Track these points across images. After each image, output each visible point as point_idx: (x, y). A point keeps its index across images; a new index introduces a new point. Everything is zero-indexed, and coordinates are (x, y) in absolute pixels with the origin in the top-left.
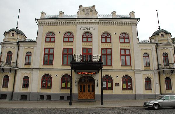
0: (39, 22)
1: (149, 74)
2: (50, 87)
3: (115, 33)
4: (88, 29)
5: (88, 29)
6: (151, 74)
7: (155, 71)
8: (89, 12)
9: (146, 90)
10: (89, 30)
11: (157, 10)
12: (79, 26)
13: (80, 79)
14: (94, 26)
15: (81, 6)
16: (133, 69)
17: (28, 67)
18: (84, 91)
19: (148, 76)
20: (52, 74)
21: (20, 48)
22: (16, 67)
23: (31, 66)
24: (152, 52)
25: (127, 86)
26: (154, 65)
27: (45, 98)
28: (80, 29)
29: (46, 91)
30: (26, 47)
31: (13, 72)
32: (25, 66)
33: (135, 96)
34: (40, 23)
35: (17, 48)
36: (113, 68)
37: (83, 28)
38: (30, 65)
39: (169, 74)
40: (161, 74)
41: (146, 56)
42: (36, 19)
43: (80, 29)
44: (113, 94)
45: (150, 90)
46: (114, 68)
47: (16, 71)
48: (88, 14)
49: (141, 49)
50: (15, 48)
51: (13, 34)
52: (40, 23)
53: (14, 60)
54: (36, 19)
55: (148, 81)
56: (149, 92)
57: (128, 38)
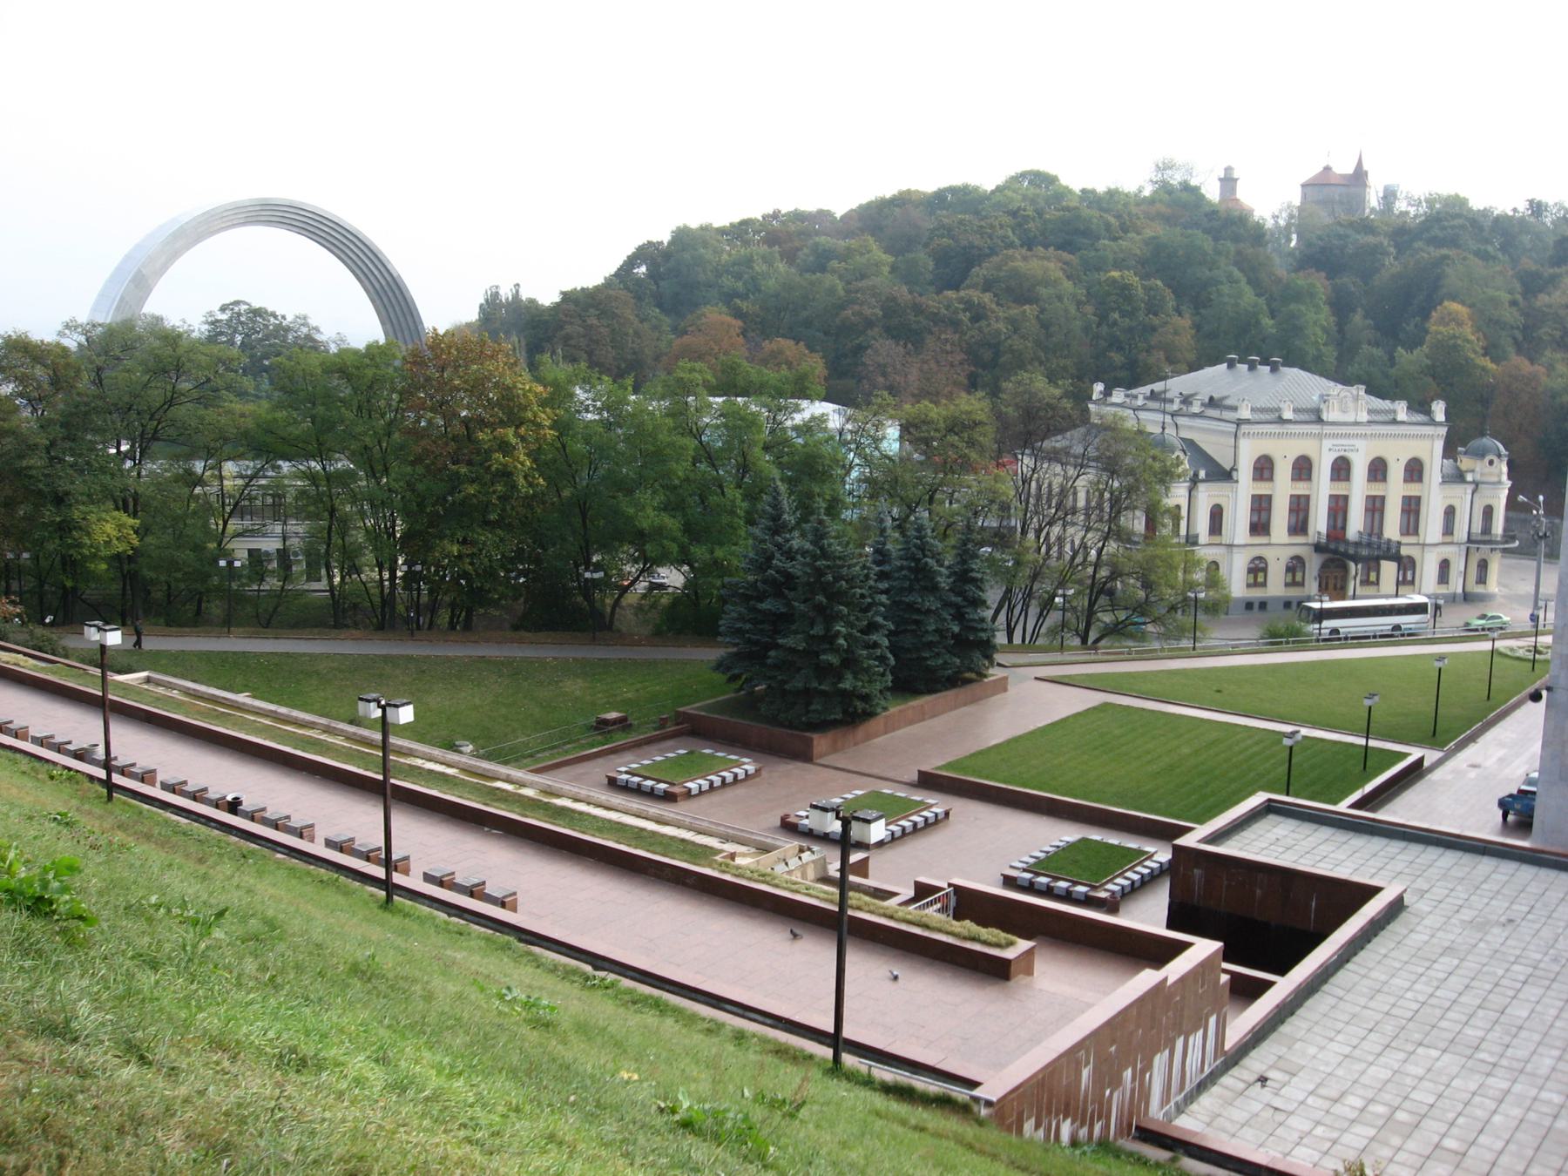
1: (1447, 552)
2: (1264, 584)
10: (1347, 454)
12: (1327, 443)
14: (1359, 443)
18: (1327, 588)
19: (1445, 556)
20: (1269, 554)
23: (1226, 539)
26: (1461, 533)
27: (1256, 606)
29: (1257, 594)
40: (1472, 551)
41: (1450, 512)
55: (1445, 565)
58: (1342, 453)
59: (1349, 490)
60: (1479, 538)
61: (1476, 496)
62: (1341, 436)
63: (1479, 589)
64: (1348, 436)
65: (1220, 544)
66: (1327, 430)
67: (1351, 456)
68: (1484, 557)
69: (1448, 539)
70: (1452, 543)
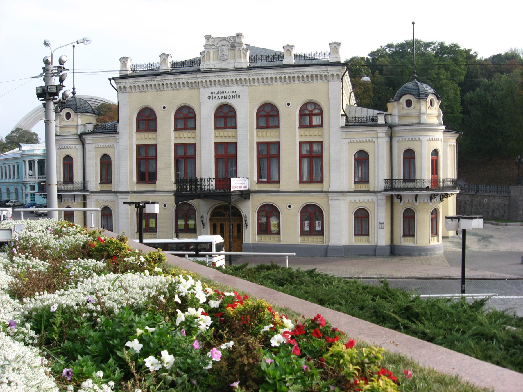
0: (118, 87)
3: (288, 104)
4: (225, 98)
5: (225, 98)
6: (370, 201)
7: (378, 194)
8: (227, 53)
9: (355, 235)
11: (413, 23)
12: (205, 92)
13: (212, 211)
14: (239, 89)
15: (208, 37)
16: (325, 189)
17: (106, 187)
21: (87, 146)
22: (85, 189)
24: (376, 149)
25: (312, 226)
28: (209, 98)
30: (102, 144)
31: (80, 200)
32: (103, 185)
33: (327, 249)
34: (120, 87)
35: (80, 147)
36: (282, 189)
37: (214, 96)
38: (111, 182)
39: (410, 201)
40: (396, 200)
42: (110, 80)
43: (209, 98)
44: (281, 243)
45: (366, 237)
46: (284, 186)
47: (84, 197)
48: (226, 57)
49: (348, 141)
50: (77, 146)
51: (68, 116)
52: (120, 87)
53: (77, 176)
54: (110, 80)
56: (362, 242)
57: (321, 114)
58: (223, 101)
59: (235, 137)
60: (402, 185)
61: (395, 140)
62: (219, 83)
63: (407, 242)
64: (228, 82)
65: (110, 192)
66: (201, 78)
67: (231, 102)
68: (409, 206)
69: (363, 187)
70: (368, 191)
